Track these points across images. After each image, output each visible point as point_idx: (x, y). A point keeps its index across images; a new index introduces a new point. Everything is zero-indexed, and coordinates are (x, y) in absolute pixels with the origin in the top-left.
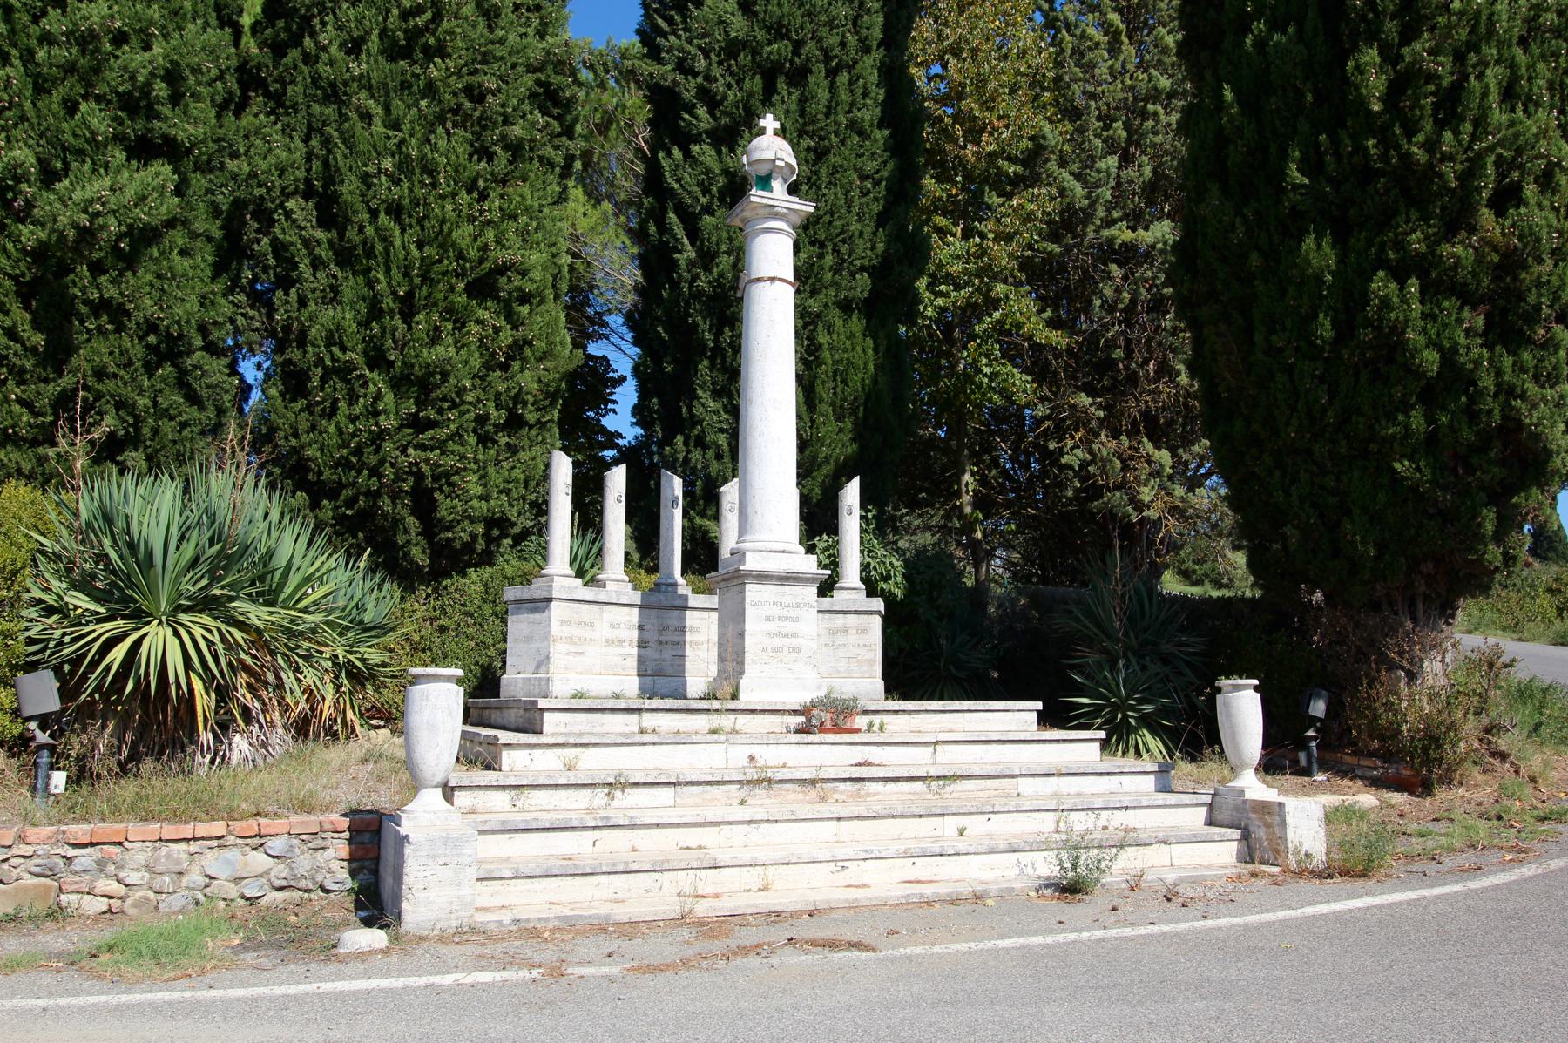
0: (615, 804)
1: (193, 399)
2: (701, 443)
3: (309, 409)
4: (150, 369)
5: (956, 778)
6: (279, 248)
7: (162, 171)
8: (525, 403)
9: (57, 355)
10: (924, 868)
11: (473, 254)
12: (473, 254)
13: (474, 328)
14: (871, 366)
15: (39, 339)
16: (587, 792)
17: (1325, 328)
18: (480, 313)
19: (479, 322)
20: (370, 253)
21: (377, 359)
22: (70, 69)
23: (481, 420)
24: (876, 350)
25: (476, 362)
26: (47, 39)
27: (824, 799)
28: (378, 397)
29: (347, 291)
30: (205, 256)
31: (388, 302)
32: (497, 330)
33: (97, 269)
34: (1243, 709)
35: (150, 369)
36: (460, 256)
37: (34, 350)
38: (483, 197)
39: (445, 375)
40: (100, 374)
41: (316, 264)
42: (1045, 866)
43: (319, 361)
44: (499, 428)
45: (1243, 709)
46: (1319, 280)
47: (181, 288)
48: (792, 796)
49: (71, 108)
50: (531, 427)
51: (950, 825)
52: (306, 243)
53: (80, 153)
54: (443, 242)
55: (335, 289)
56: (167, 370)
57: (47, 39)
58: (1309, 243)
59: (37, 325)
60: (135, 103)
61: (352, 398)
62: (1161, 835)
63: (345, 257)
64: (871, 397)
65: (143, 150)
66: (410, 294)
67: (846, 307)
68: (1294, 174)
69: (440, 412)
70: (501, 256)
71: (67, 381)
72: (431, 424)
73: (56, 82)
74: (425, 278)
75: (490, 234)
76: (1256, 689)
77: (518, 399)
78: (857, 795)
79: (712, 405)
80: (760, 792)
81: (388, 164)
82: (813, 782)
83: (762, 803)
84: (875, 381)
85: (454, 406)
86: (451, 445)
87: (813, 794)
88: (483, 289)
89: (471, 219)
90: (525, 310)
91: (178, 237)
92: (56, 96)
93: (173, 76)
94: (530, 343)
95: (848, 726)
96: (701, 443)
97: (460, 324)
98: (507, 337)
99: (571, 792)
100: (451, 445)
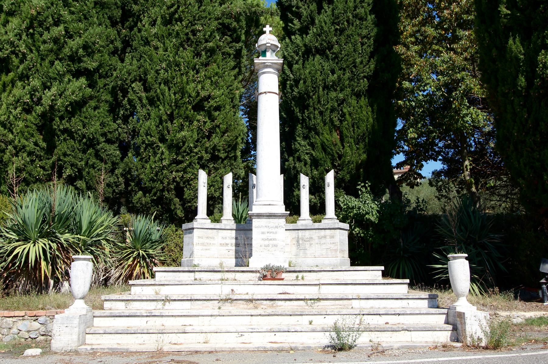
0: (166, 307)
1: (102, 160)
2: (299, 159)
3: (141, 160)
4: (84, 152)
5: (319, 299)
6: (130, 101)
7: (83, 80)
8: (219, 151)
9: (50, 150)
10: (280, 337)
11: (194, 94)
12: (194, 94)
13: (195, 123)
14: (371, 120)
15: (44, 145)
16: (155, 303)
17: (522, 81)
18: (199, 117)
19: (198, 121)
20: (159, 99)
21: (163, 140)
22: (51, 51)
23: (201, 158)
24: (373, 112)
25: (195, 136)
26: (44, 42)
27: (256, 308)
28: (162, 153)
29: (153, 115)
30: (104, 107)
31: (165, 117)
32: (205, 123)
33: (62, 118)
34: (460, 268)
35: (84, 152)
36: (190, 96)
37: (43, 149)
38: (198, 72)
39: (184, 143)
40: (65, 155)
41: (143, 106)
42: (325, 339)
43: (143, 142)
44: (208, 161)
45: (460, 268)
46: (518, 59)
47: (95, 121)
48: (242, 306)
49: (52, 63)
50: (223, 160)
51: (306, 319)
52: (140, 99)
53: (55, 79)
54: (182, 92)
55: (149, 114)
56: (91, 151)
57: (44, 42)
58: (511, 41)
59: (44, 140)
60: (74, 58)
61: (155, 154)
62: (405, 327)
63: (152, 102)
64: (373, 132)
65: (77, 74)
66: (172, 113)
67: (358, 95)
68: (504, 10)
69: (183, 157)
70: (203, 94)
71: (54, 158)
72: (181, 162)
73: (47, 56)
74: (176, 106)
75: (200, 86)
76: (466, 258)
77: (214, 148)
78: (272, 306)
79: (303, 143)
80: (228, 304)
81: (164, 65)
82: (251, 300)
83: (227, 308)
84: (373, 126)
85: (188, 154)
86: (189, 169)
87: (251, 305)
88: (198, 107)
89: (194, 81)
90: (217, 113)
91: (93, 103)
92: (47, 61)
93: (85, 47)
94: (219, 127)
95: (278, 277)
96: (299, 159)
97: (191, 122)
98: (209, 125)
99: (149, 303)
100: (189, 169)
